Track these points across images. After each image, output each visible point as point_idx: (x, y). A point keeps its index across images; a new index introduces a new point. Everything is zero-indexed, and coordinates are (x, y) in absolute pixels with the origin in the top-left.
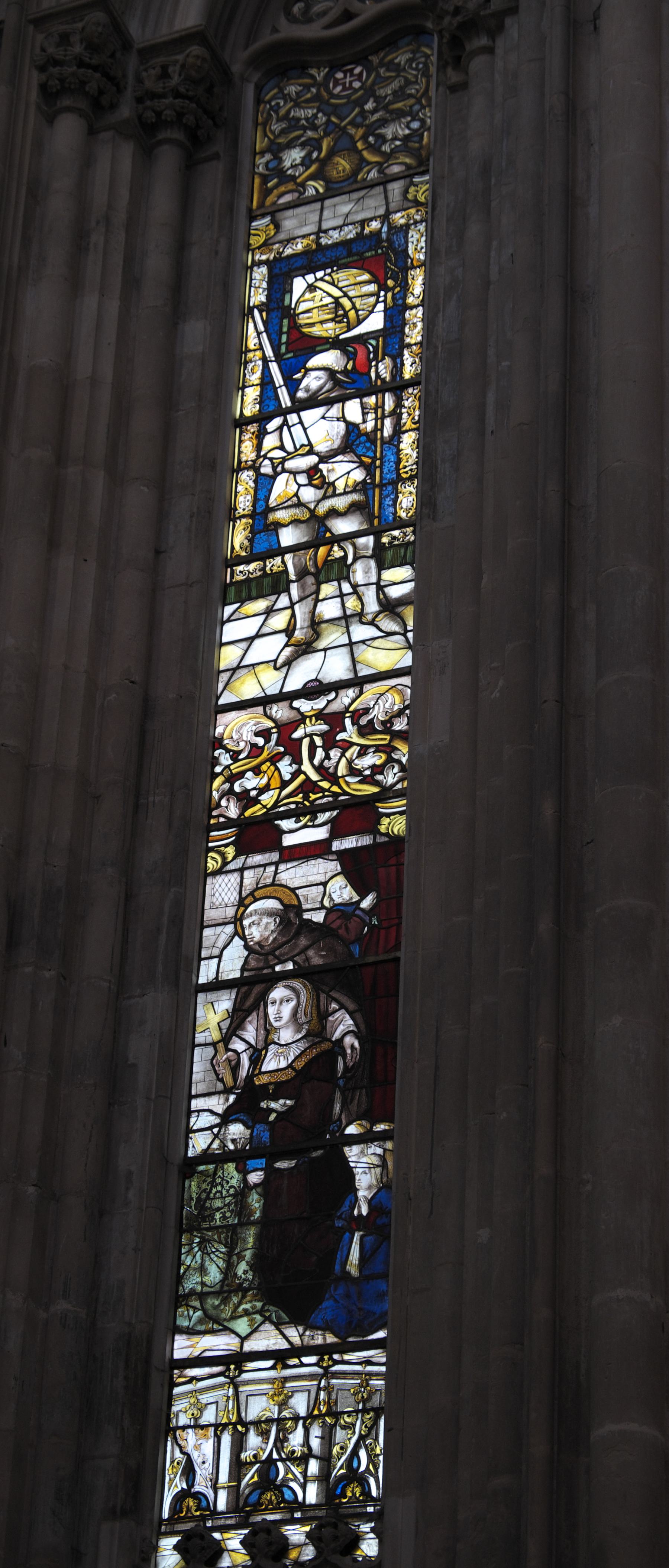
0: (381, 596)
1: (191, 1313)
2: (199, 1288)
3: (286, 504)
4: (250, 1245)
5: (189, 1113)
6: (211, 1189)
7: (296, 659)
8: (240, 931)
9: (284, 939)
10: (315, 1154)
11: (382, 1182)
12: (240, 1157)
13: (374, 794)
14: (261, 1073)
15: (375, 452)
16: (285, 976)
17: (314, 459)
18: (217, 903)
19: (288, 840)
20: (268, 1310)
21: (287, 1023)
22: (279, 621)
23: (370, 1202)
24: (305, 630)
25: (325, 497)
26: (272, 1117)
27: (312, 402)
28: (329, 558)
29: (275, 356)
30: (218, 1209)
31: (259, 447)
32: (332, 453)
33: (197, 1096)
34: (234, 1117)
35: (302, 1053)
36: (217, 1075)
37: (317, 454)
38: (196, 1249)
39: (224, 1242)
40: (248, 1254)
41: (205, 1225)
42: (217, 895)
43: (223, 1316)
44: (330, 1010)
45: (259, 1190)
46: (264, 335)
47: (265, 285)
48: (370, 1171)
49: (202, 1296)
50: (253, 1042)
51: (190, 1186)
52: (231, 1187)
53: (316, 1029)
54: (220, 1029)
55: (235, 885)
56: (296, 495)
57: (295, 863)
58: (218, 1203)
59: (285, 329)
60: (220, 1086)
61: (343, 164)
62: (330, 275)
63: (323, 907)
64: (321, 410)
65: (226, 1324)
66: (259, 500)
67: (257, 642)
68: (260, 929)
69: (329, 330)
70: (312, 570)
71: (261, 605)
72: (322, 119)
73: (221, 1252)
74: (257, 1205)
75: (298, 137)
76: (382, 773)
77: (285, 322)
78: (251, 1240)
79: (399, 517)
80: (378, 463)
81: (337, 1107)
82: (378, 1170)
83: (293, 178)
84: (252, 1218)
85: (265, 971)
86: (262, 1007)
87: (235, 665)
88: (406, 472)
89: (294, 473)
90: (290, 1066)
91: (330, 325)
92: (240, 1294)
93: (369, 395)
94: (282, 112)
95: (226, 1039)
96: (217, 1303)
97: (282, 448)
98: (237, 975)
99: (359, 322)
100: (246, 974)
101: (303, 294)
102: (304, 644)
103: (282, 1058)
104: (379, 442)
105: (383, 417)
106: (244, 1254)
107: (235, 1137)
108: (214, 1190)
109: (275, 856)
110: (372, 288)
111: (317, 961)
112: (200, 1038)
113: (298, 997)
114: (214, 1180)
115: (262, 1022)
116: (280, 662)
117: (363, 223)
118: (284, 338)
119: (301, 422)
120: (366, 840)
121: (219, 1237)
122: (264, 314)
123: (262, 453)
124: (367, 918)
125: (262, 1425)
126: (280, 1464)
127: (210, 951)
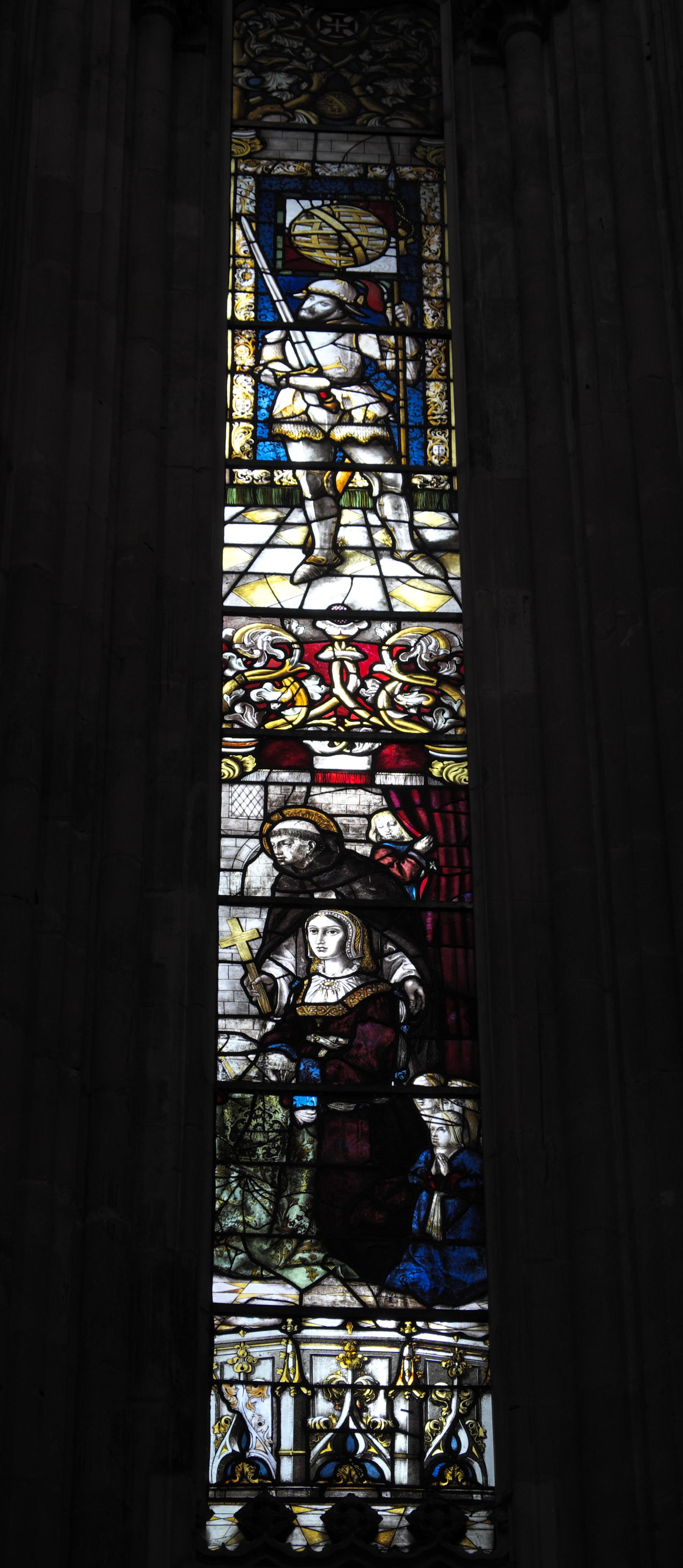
0: (416, 537)
1: (233, 1254)
2: (241, 1228)
3: (294, 419)
4: (303, 1189)
5: (218, 1034)
7: (317, 578)
8: (267, 848)
9: (323, 866)
10: (378, 1101)
11: (463, 1142)
12: (287, 1091)
13: (422, 734)
15: (398, 392)
16: (326, 905)
17: (324, 383)
18: (237, 813)
19: (321, 763)
20: (331, 1264)
21: (333, 955)
22: (296, 535)
24: (326, 551)
25: (340, 423)
26: (323, 1053)
27: (319, 323)
28: (350, 485)
29: (269, 269)
30: (260, 1144)
31: (257, 355)
32: (346, 381)
33: (225, 1016)
34: (274, 1046)
36: (250, 997)
37: (328, 378)
38: (234, 1184)
39: (270, 1181)
40: (301, 1198)
41: (243, 1159)
42: (236, 804)
43: (275, 1262)
45: (311, 1130)
46: (256, 245)
47: (252, 196)
48: (448, 1129)
49: (246, 1238)
50: (292, 970)
51: (223, 1113)
52: (276, 1122)
54: (250, 949)
55: (258, 798)
56: (305, 413)
57: (332, 789)
58: (260, 1138)
59: (280, 246)
60: (254, 1010)
61: (337, 105)
62: (328, 206)
63: (368, 841)
64: (331, 336)
65: (278, 1272)
66: (261, 408)
67: (266, 552)
69: (332, 259)
70: (331, 492)
71: (271, 515)
72: (309, 54)
73: (266, 1192)
74: (309, 1146)
75: (284, 64)
76: (430, 715)
77: (280, 239)
78: (304, 1183)
79: (431, 462)
80: (401, 403)
81: (403, 1055)
83: (279, 102)
84: (304, 1160)
85: (301, 896)
86: (300, 934)
87: (242, 569)
88: (436, 420)
89: (302, 390)
90: (340, 1002)
91: (334, 255)
92: (294, 1242)
93: (388, 334)
94: (263, 34)
96: (265, 1247)
97: (285, 361)
98: (268, 894)
99: (368, 261)
100: (277, 895)
101: (298, 217)
102: (325, 565)
103: (330, 991)
104: (401, 383)
105: (405, 360)
106: (296, 1197)
107: (276, 1068)
108: (254, 1123)
109: (306, 778)
110: (380, 231)
111: (364, 895)
112: (223, 954)
114: (253, 1111)
115: (302, 949)
116: (297, 577)
117: (366, 166)
118: (279, 255)
119: (307, 341)
120: (415, 781)
121: (263, 1175)
122: (254, 225)
123: (262, 362)
124: (423, 862)
125: (333, 1391)
126: (359, 1436)
127: (231, 863)
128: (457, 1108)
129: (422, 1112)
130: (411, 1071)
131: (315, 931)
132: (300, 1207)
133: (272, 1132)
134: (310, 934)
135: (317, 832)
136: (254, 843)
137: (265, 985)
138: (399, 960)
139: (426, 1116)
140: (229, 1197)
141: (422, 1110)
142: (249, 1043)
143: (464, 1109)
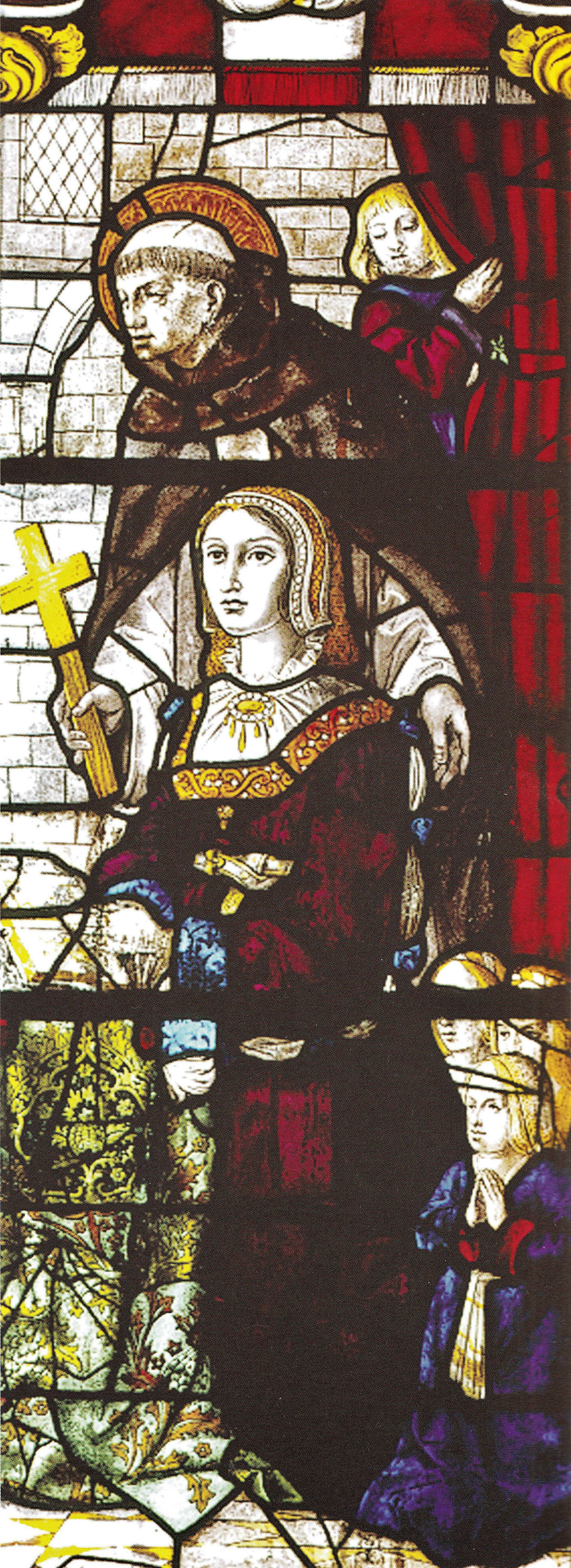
1: (29, 1446)
2: (47, 1378)
6: (65, 1095)
8: (109, 308)
14: (190, 764)
18: (38, 208)
19: (242, 43)
20: (244, 1466)
23: (510, 1193)
26: (231, 905)
30: (89, 1157)
34: (121, 888)
35: (310, 722)
36: (69, 753)
38: (34, 1263)
39: (110, 1254)
40: (180, 1294)
41: (52, 1197)
42: (36, 179)
43: (119, 1465)
44: (383, 605)
45: (201, 1114)
50: (167, 668)
52: (122, 1095)
53: (347, 661)
57: (263, 121)
60: (78, 790)
63: (350, 279)
65: (128, 1488)
68: (174, 316)
81: (413, 901)
82: (530, 1103)
84: (187, 1194)
86: (186, 562)
90: (274, 756)
92: (163, 1407)
95: (87, 645)
96: (100, 1427)
103: (250, 728)
107: (128, 948)
108: (74, 1100)
109: (203, 88)
113: (290, 550)
114: (72, 1068)
115: (188, 606)
120: (467, 90)
121: (96, 1238)
128: (531, 1048)
129: (449, 1060)
130: (433, 950)
131: (220, 554)
132: (177, 1319)
133: (115, 1122)
134: (208, 562)
135: (230, 258)
136: (79, 293)
137: (103, 715)
138: (412, 634)
139: (458, 1068)
140: (23, 1299)
141: (451, 1053)
142: (65, 880)
143: (545, 1047)
